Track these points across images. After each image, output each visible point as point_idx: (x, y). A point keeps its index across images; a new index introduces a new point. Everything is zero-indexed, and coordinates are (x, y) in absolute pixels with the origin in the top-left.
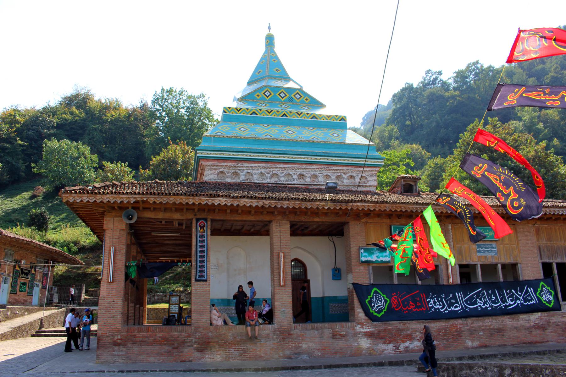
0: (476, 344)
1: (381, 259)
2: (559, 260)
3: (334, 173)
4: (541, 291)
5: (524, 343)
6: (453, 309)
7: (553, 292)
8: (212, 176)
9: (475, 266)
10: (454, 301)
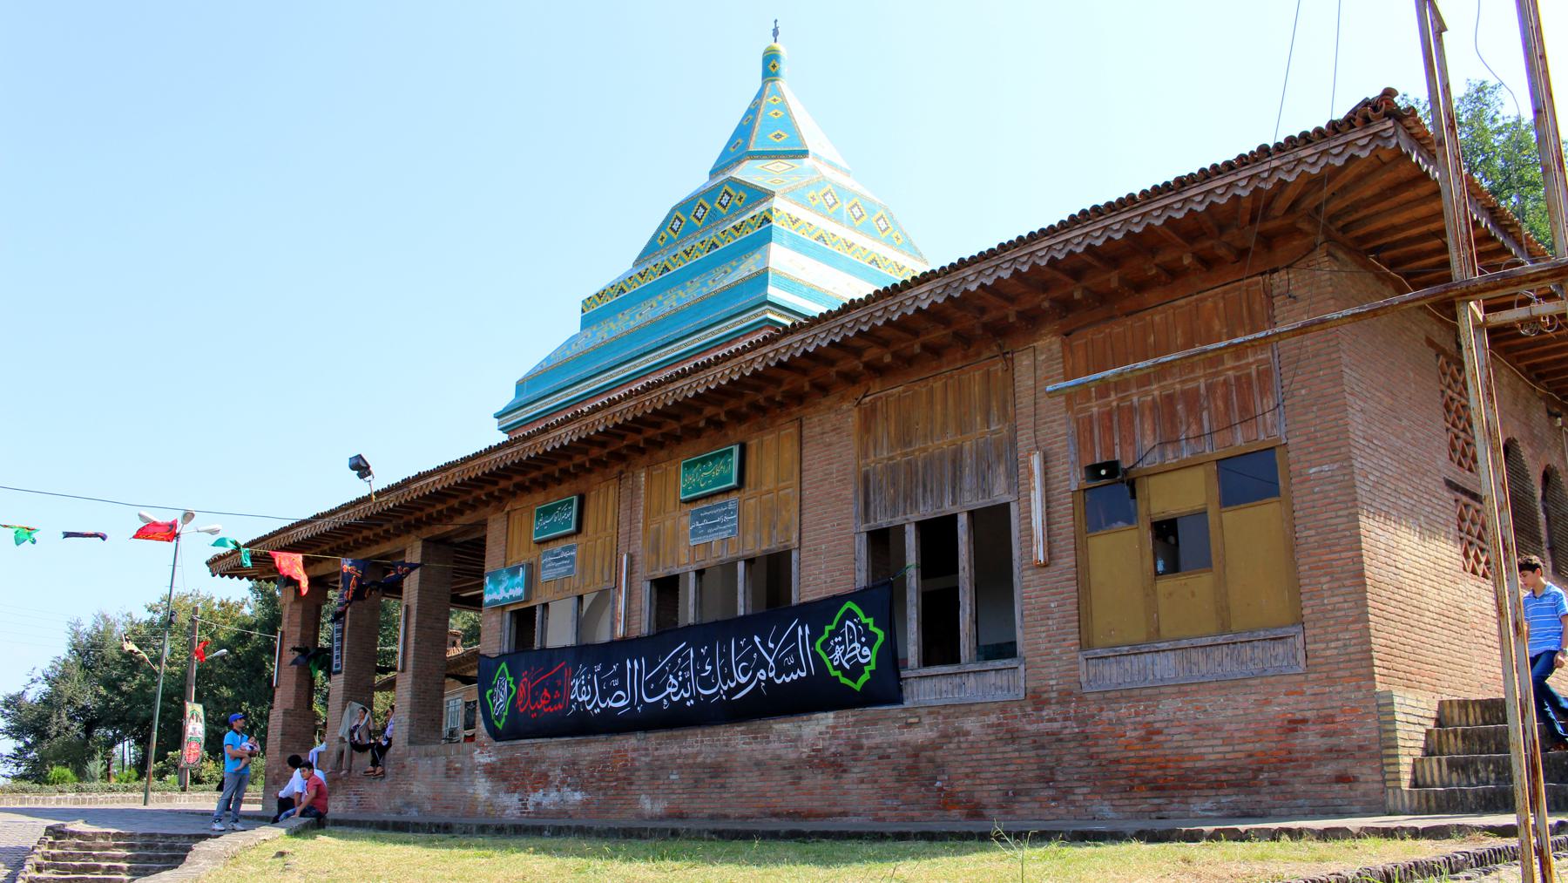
0: (659, 807)
2: (927, 511)
4: (833, 634)
5: (775, 815)
6: (611, 704)
7: (881, 635)
10: (616, 683)
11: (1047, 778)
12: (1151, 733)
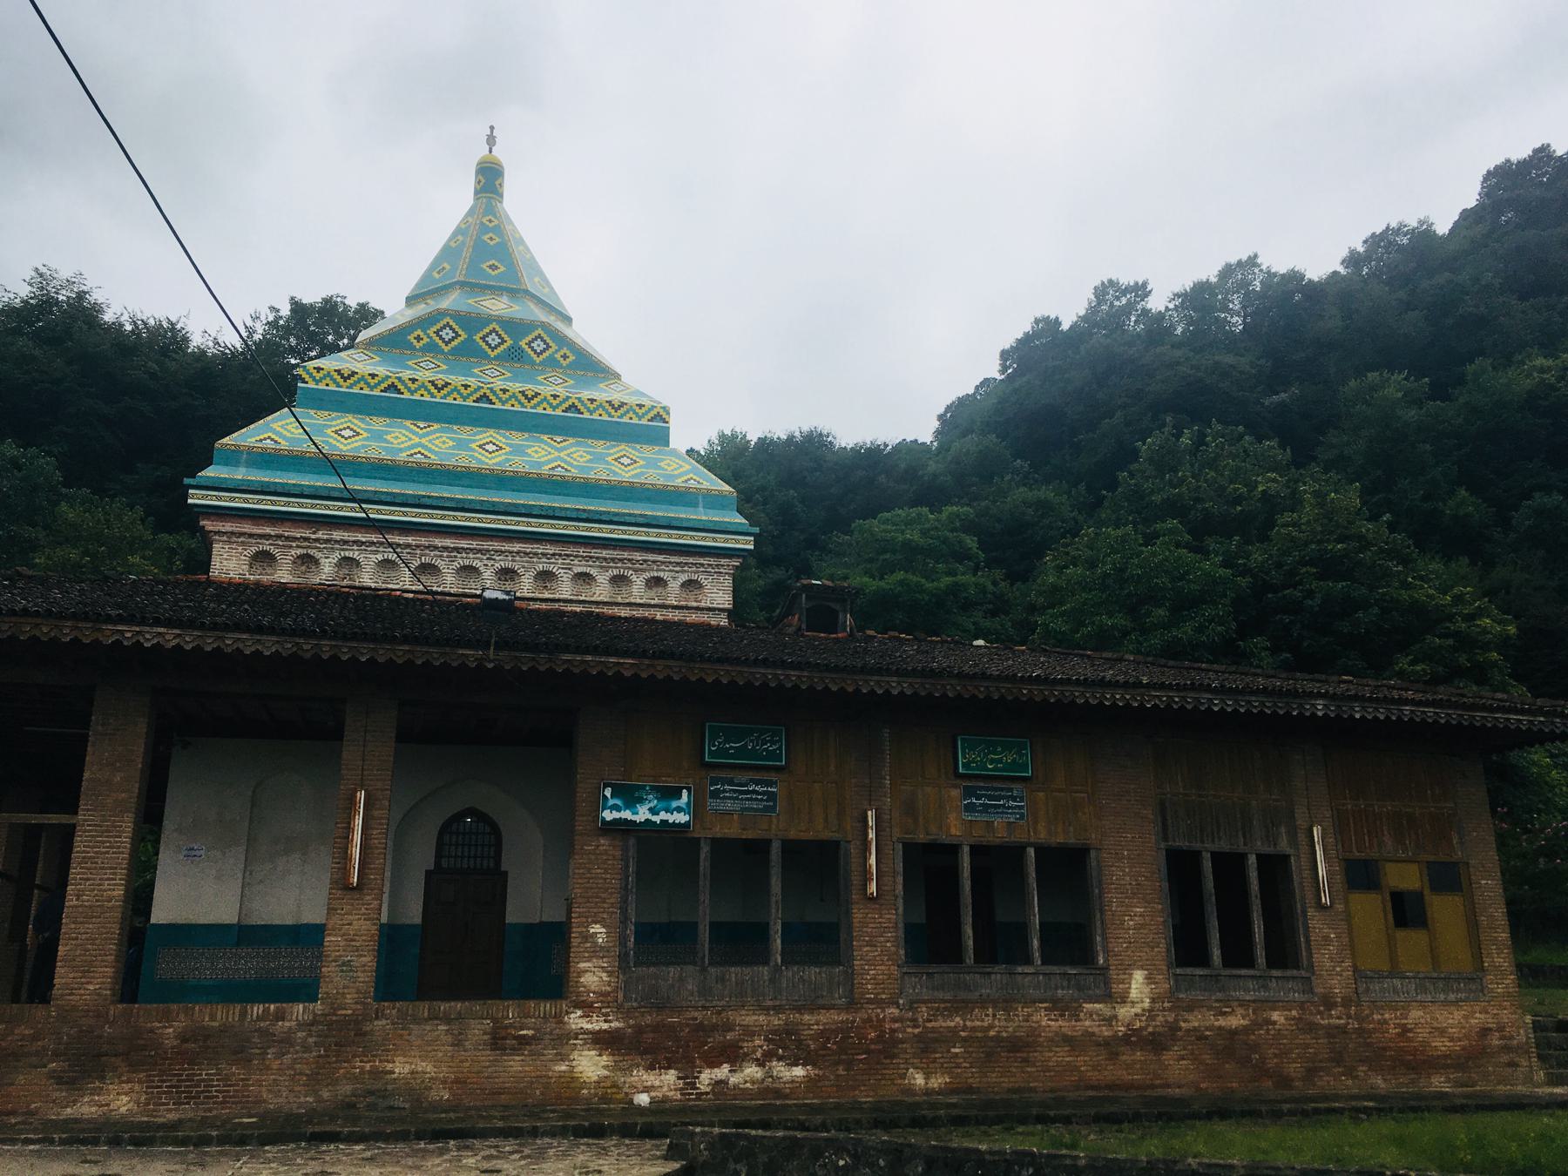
0: (937, 1082)
1: (663, 816)
2: (1223, 845)
3: (606, 569)
8: (232, 564)
9: (953, 849)
11: (1338, 1059)
12: (1405, 1030)
